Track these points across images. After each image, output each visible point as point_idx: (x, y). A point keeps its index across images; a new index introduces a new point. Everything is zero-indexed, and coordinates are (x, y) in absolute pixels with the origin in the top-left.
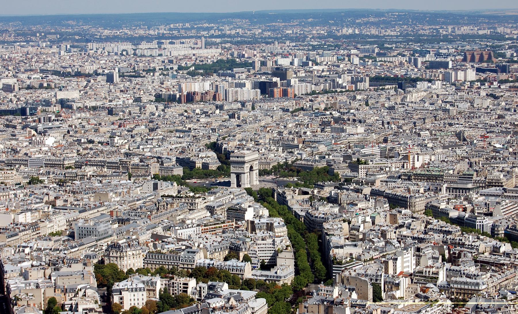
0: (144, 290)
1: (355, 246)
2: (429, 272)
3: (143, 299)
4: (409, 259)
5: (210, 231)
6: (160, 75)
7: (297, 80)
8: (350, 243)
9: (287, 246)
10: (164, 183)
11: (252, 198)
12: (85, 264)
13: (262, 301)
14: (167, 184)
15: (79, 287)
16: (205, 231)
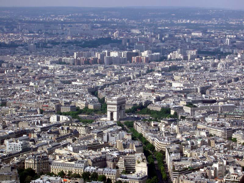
2: (234, 177)
5: (93, 149)
11: (120, 128)
14: (66, 117)
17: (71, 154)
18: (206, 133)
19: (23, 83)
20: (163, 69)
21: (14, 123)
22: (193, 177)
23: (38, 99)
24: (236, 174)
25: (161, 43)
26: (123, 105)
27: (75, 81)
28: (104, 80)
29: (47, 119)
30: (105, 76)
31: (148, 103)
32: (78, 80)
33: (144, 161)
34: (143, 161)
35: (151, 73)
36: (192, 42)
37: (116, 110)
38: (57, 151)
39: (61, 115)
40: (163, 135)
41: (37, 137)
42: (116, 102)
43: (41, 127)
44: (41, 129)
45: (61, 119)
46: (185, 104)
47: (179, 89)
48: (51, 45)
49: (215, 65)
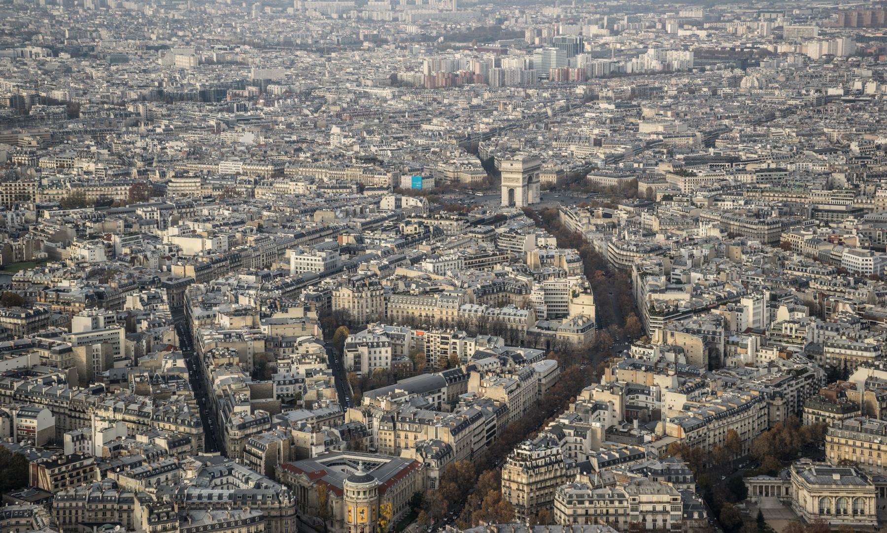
0: (389, 346)
1: (681, 290)
2: (791, 329)
3: (387, 358)
4: (761, 310)
6: (396, 48)
7: (590, 56)
8: (674, 286)
9: (586, 289)
10: (411, 199)
11: (532, 221)
12: (307, 309)
13: (552, 363)
15: (299, 339)
16: (469, 266)
17: (429, 279)
18: (722, 231)
19: (315, 127)
20: (619, 94)
21: (304, 212)
22: (695, 327)
23: (351, 162)
24: (794, 322)
25: (611, 38)
26: (536, 173)
27: (429, 121)
28: (491, 121)
29: (375, 203)
30: (491, 112)
31: (589, 167)
32: (435, 121)
33: (589, 291)
34: (585, 292)
35: (590, 104)
36: (681, 33)
37: (521, 184)
38: (400, 271)
39: (403, 195)
40: (624, 238)
41: (355, 242)
42: (519, 166)
43: (363, 220)
44: (363, 224)
45: (404, 205)
46: (671, 169)
47: (654, 137)
48: (371, 45)
49: (735, 82)
